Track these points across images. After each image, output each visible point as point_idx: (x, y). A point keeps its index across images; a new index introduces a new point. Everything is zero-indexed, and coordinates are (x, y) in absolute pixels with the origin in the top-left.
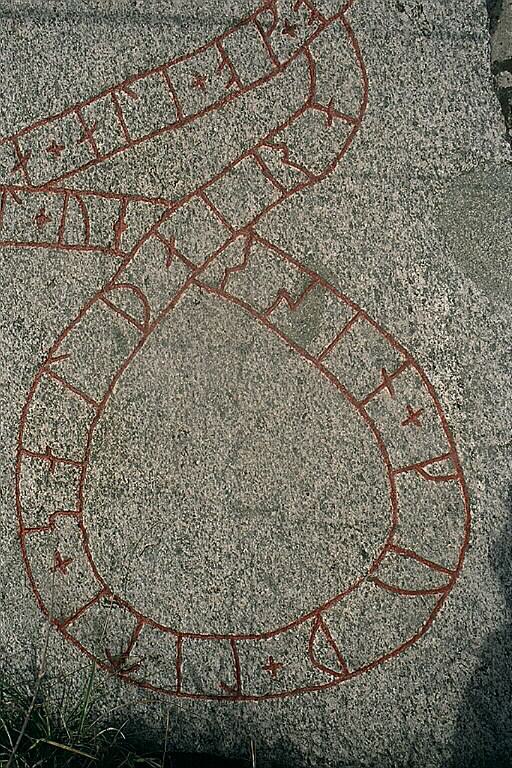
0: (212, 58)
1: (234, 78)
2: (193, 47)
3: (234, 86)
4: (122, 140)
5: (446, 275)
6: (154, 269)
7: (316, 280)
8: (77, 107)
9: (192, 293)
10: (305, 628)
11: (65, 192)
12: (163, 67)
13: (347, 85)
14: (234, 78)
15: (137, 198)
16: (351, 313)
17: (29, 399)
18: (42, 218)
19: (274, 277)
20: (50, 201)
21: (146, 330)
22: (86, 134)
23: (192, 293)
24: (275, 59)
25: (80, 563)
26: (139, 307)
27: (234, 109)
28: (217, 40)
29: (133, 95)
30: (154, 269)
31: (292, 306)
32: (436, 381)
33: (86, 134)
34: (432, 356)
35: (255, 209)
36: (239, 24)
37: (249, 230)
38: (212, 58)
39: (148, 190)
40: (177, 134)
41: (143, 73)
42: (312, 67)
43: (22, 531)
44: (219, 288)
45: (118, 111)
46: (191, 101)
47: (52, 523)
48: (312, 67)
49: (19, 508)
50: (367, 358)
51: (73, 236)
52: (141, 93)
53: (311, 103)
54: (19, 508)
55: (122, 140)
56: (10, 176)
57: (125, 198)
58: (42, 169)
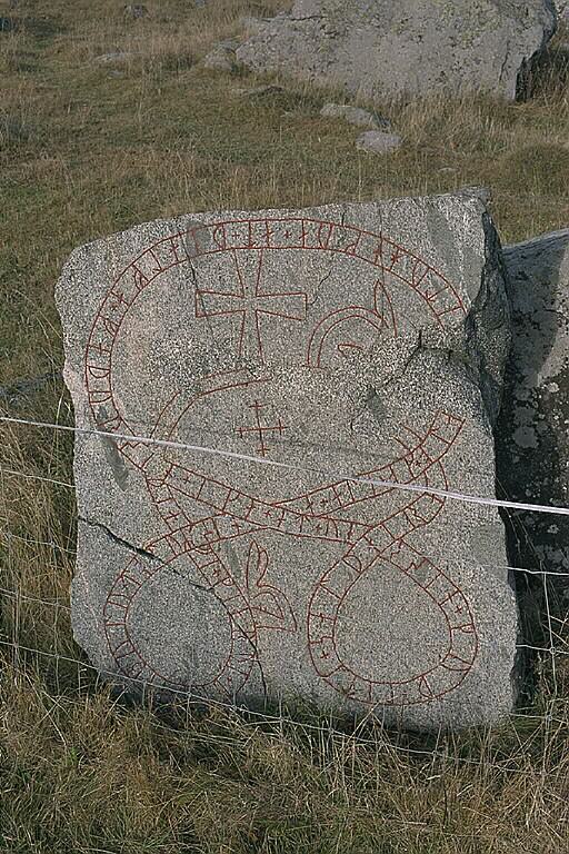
6: (364, 550)
9: (378, 560)
19: (411, 557)
23: (378, 560)
26: (358, 564)
30: (364, 550)
31: (416, 568)
33: (337, 497)
35: (403, 533)
36: (399, 460)
37: (401, 540)
57: (352, 523)
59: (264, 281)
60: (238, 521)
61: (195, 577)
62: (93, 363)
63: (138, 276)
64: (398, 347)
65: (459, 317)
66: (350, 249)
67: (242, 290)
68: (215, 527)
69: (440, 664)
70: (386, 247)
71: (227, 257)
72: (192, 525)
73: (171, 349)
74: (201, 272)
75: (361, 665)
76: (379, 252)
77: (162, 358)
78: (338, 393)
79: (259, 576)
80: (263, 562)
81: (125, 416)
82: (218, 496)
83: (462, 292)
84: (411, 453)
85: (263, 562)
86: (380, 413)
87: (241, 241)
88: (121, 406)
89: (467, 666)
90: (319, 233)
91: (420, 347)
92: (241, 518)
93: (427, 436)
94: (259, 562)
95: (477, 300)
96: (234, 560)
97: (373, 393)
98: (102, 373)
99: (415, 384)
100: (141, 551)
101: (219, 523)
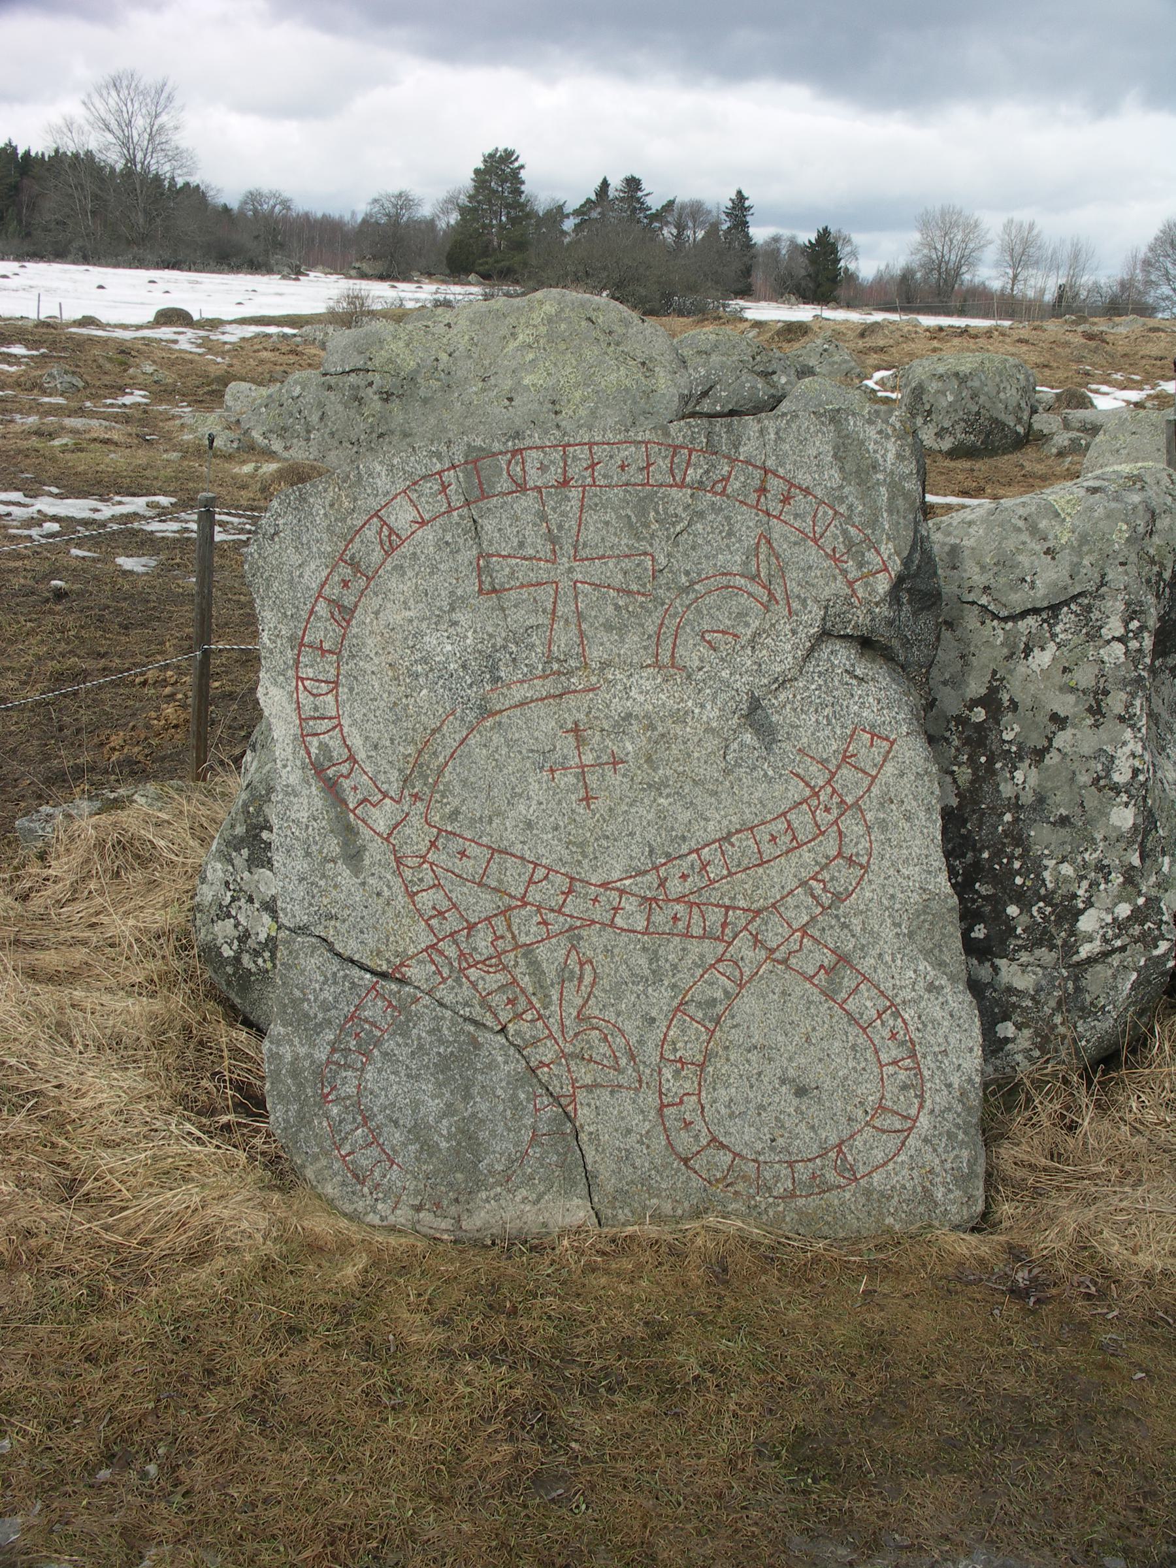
0: (781, 825)
1: (795, 838)
2: (769, 817)
3: (795, 844)
4: (725, 872)
5: (913, 959)
6: (743, 947)
7: (843, 959)
8: (697, 851)
10: (832, 1155)
11: (691, 905)
12: (751, 829)
13: (860, 847)
14: (795, 838)
15: (735, 908)
16: (860, 978)
17: (668, 1028)
18: (675, 919)
20: (680, 908)
21: (741, 986)
22: (704, 867)
24: (818, 827)
25: (699, 1125)
26: (737, 973)
27: (794, 857)
28: (784, 814)
29: (733, 845)
32: (906, 1016)
34: (904, 1002)
35: (806, 918)
37: (803, 930)
38: (781, 825)
39: (742, 904)
40: (760, 870)
41: (738, 831)
42: (840, 833)
43: (663, 1106)
44: (784, 962)
45: (723, 853)
46: (768, 850)
47: (681, 1102)
48: (840, 833)
49: (661, 1093)
50: (869, 1004)
51: (696, 931)
52: (737, 844)
53: (840, 854)
54: (661, 1093)
55: (725, 872)
56: (654, 893)
57: (728, 908)
58: (675, 887)
59: (590, 535)
60: (551, 916)
61: (477, 1012)
62: (310, 673)
63: (385, 528)
64: (794, 632)
65: (883, 585)
66: (719, 487)
67: (554, 551)
68: (509, 927)
69: (867, 1124)
70: (774, 484)
71: (528, 501)
72: (471, 927)
73: (440, 645)
74: (488, 525)
75: (743, 1136)
76: (762, 490)
77: (424, 661)
78: (702, 706)
79: (580, 1002)
80: (588, 979)
81: (361, 755)
82: (514, 878)
83: (887, 548)
84: (817, 794)
85: (588, 979)
86: (766, 732)
87: (554, 475)
88: (356, 741)
89: (909, 1124)
90: (672, 462)
91: (826, 634)
92: (552, 910)
93: (839, 767)
94: (581, 979)
95: (906, 563)
96: (540, 985)
97: (755, 705)
98: (324, 687)
99: (819, 688)
100: (384, 975)
101: (516, 921)
